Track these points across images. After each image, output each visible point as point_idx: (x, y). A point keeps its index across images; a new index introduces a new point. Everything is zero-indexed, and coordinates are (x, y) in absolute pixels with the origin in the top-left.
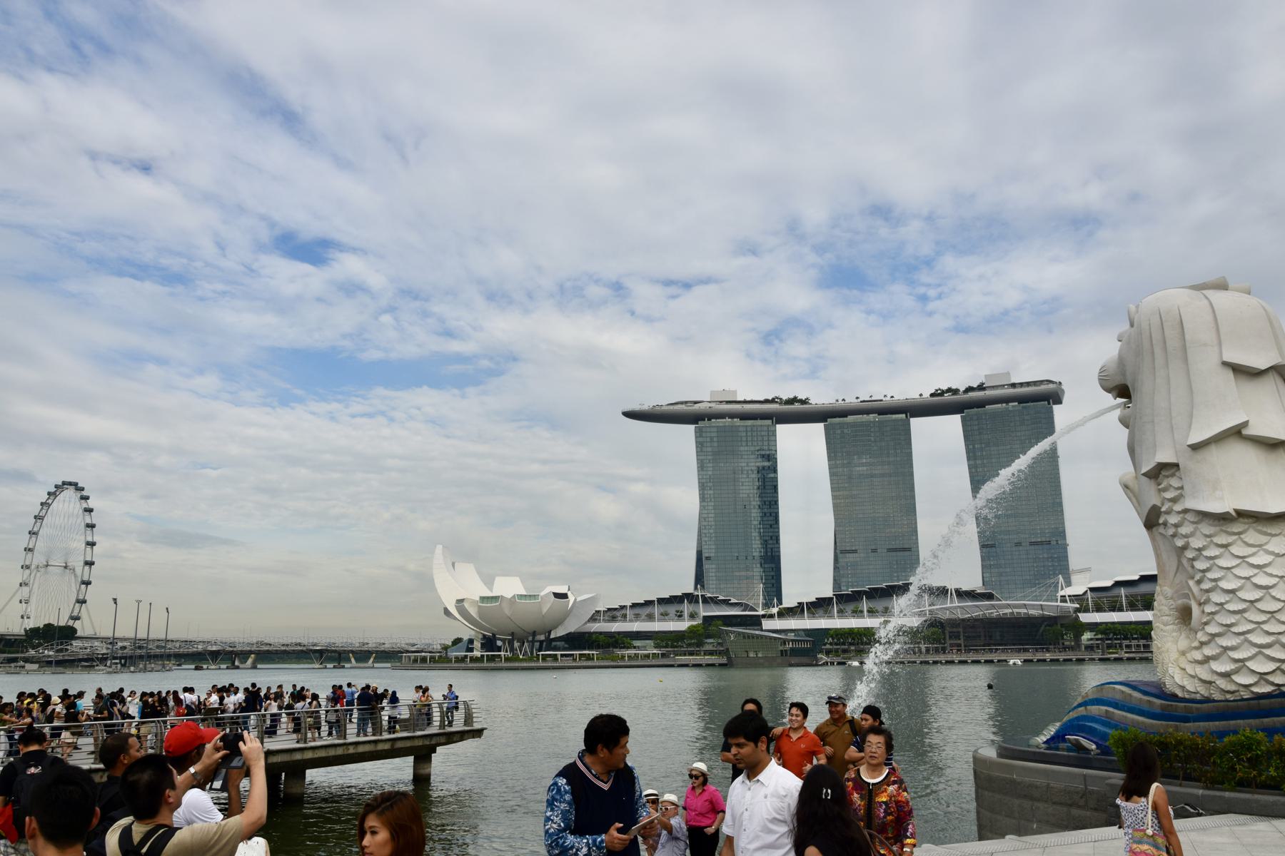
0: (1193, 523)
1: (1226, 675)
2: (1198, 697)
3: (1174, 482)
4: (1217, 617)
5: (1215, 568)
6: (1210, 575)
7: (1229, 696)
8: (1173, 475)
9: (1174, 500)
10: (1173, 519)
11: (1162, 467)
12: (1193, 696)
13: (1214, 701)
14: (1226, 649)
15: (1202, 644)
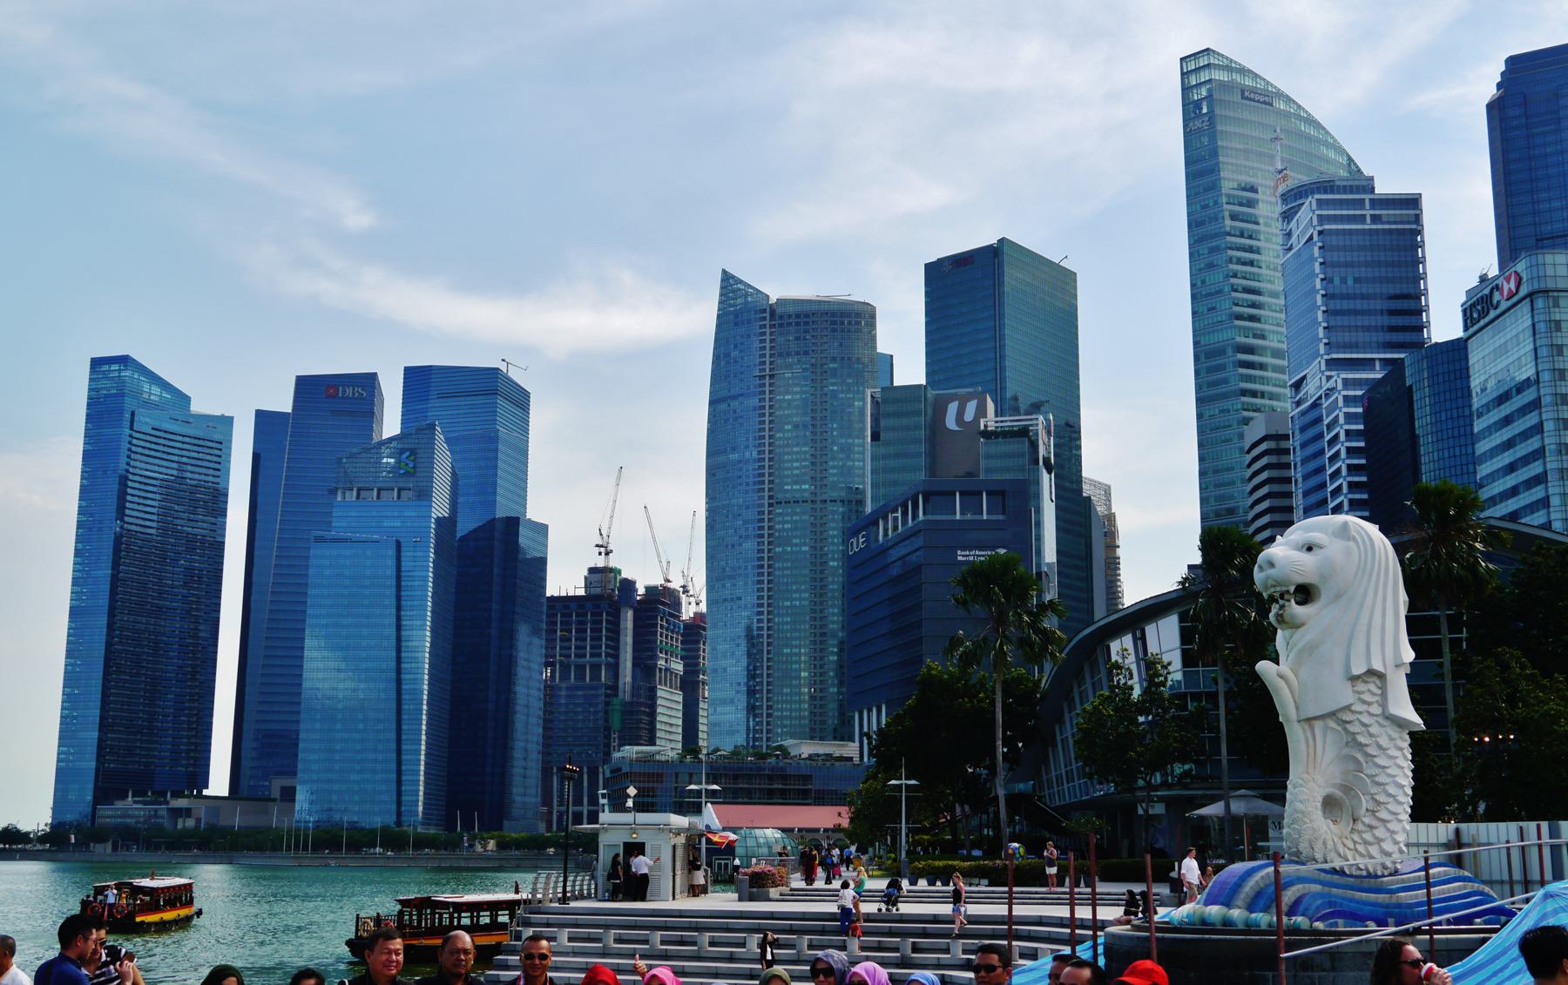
0: (1380, 725)
1: (1388, 854)
2: (1364, 873)
3: (1372, 687)
4: (1388, 806)
5: (1394, 767)
6: (1389, 771)
7: (1386, 873)
8: (1374, 682)
9: (1369, 704)
10: (1366, 719)
11: (1371, 672)
12: (1359, 873)
13: (1376, 876)
14: (1393, 832)
15: (1371, 827)
